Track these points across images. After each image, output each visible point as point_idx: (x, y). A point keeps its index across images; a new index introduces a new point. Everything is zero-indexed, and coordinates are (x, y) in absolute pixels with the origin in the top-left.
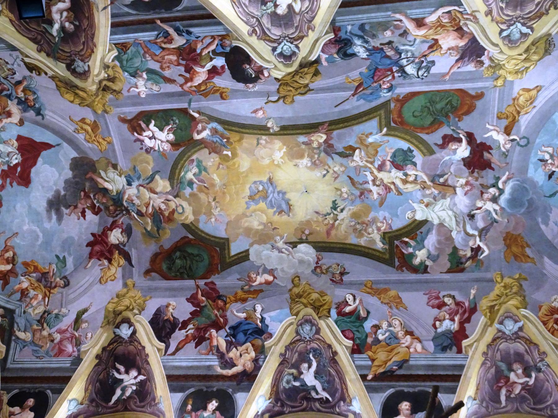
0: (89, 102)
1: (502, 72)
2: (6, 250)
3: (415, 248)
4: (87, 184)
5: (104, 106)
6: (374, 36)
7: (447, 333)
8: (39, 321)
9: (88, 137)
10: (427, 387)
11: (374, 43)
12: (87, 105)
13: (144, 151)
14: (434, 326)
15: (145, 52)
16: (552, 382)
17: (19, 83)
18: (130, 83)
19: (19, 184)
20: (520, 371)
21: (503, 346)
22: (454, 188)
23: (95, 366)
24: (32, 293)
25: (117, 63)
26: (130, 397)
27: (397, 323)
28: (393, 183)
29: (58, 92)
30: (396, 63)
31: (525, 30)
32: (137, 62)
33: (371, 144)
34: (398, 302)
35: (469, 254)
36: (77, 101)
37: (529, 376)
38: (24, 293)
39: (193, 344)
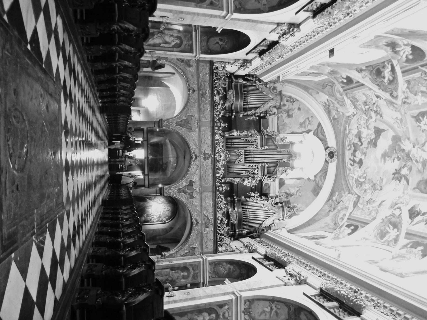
0: (398, 110)
2: (364, 173)
4: (397, 147)
5: (405, 110)
8: (367, 202)
9: (399, 125)
12: (398, 111)
13: (421, 131)
15: (418, 83)
17: (374, 104)
18: (414, 99)
19: (373, 147)
23: (382, 223)
24: (368, 191)
25: (408, 90)
26: (391, 241)
29: (387, 106)
32: (416, 88)
36: (394, 109)
38: (366, 190)
39: (424, 223)
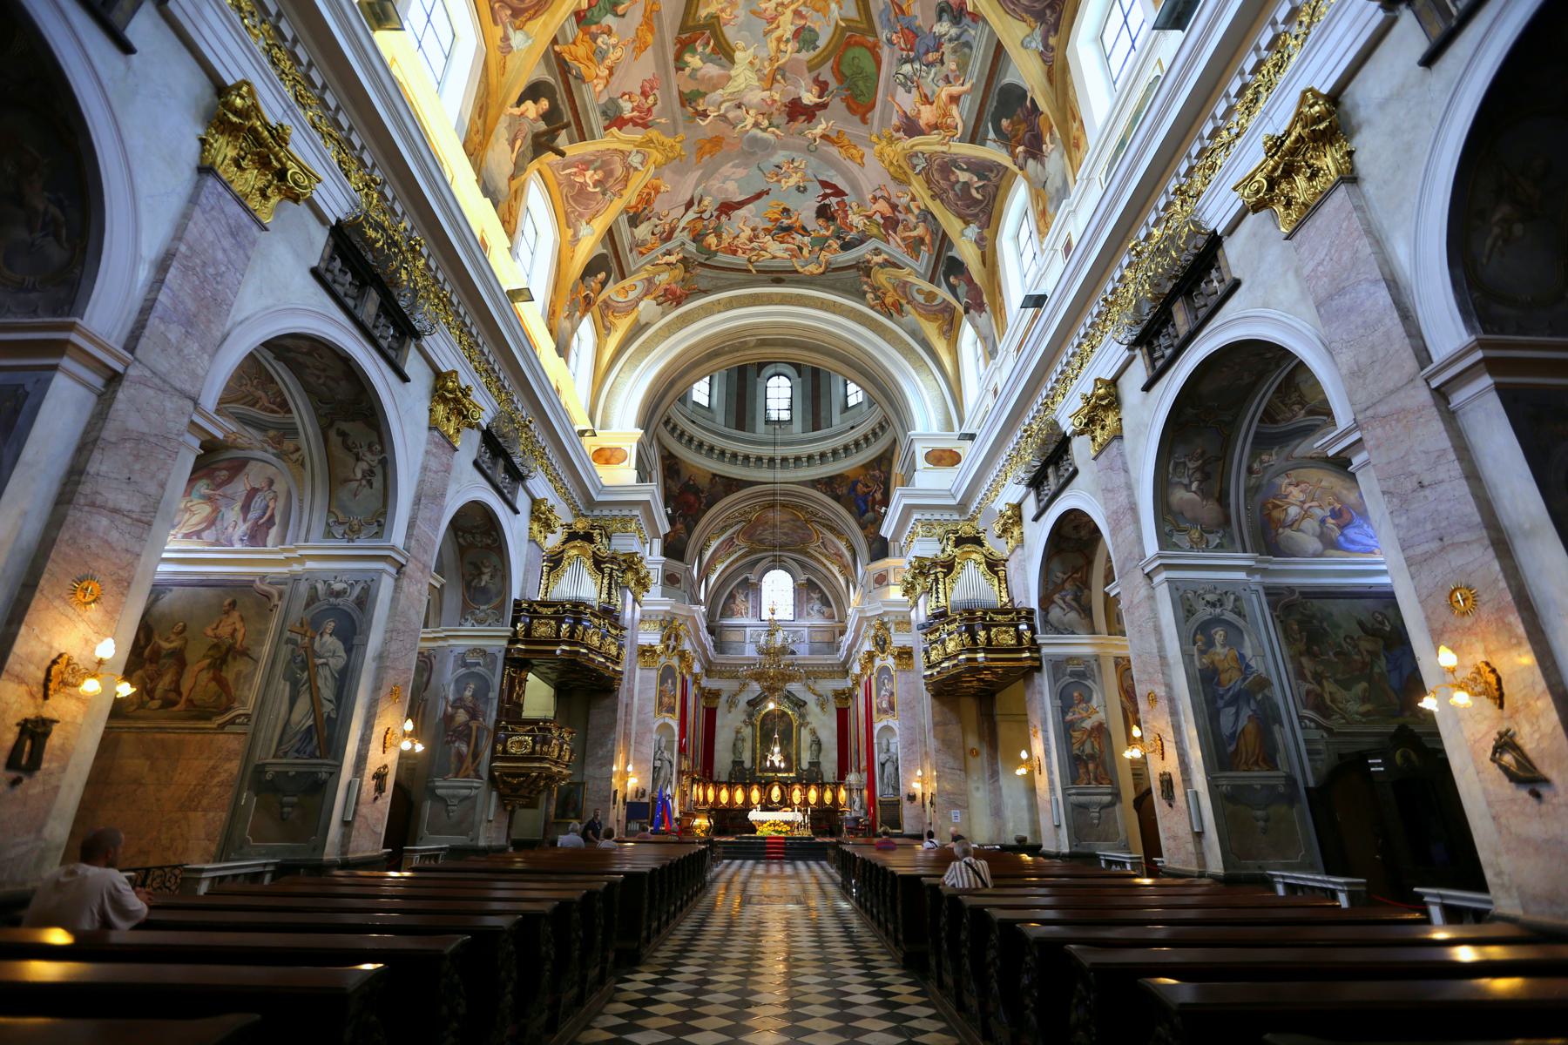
1: (884, 143)
3: (702, 54)
6: (955, 51)
7: (619, 108)
10: (568, 116)
11: (947, 48)
14: (624, 94)
16: (598, 207)
20: (596, 177)
21: (617, 159)
22: (770, 89)
27: (619, 54)
28: (778, 27)
30: (917, 58)
31: (918, 169)
33: (828, 5)
34: (640, 47)
35: (700, 108)
37: (595, 186)
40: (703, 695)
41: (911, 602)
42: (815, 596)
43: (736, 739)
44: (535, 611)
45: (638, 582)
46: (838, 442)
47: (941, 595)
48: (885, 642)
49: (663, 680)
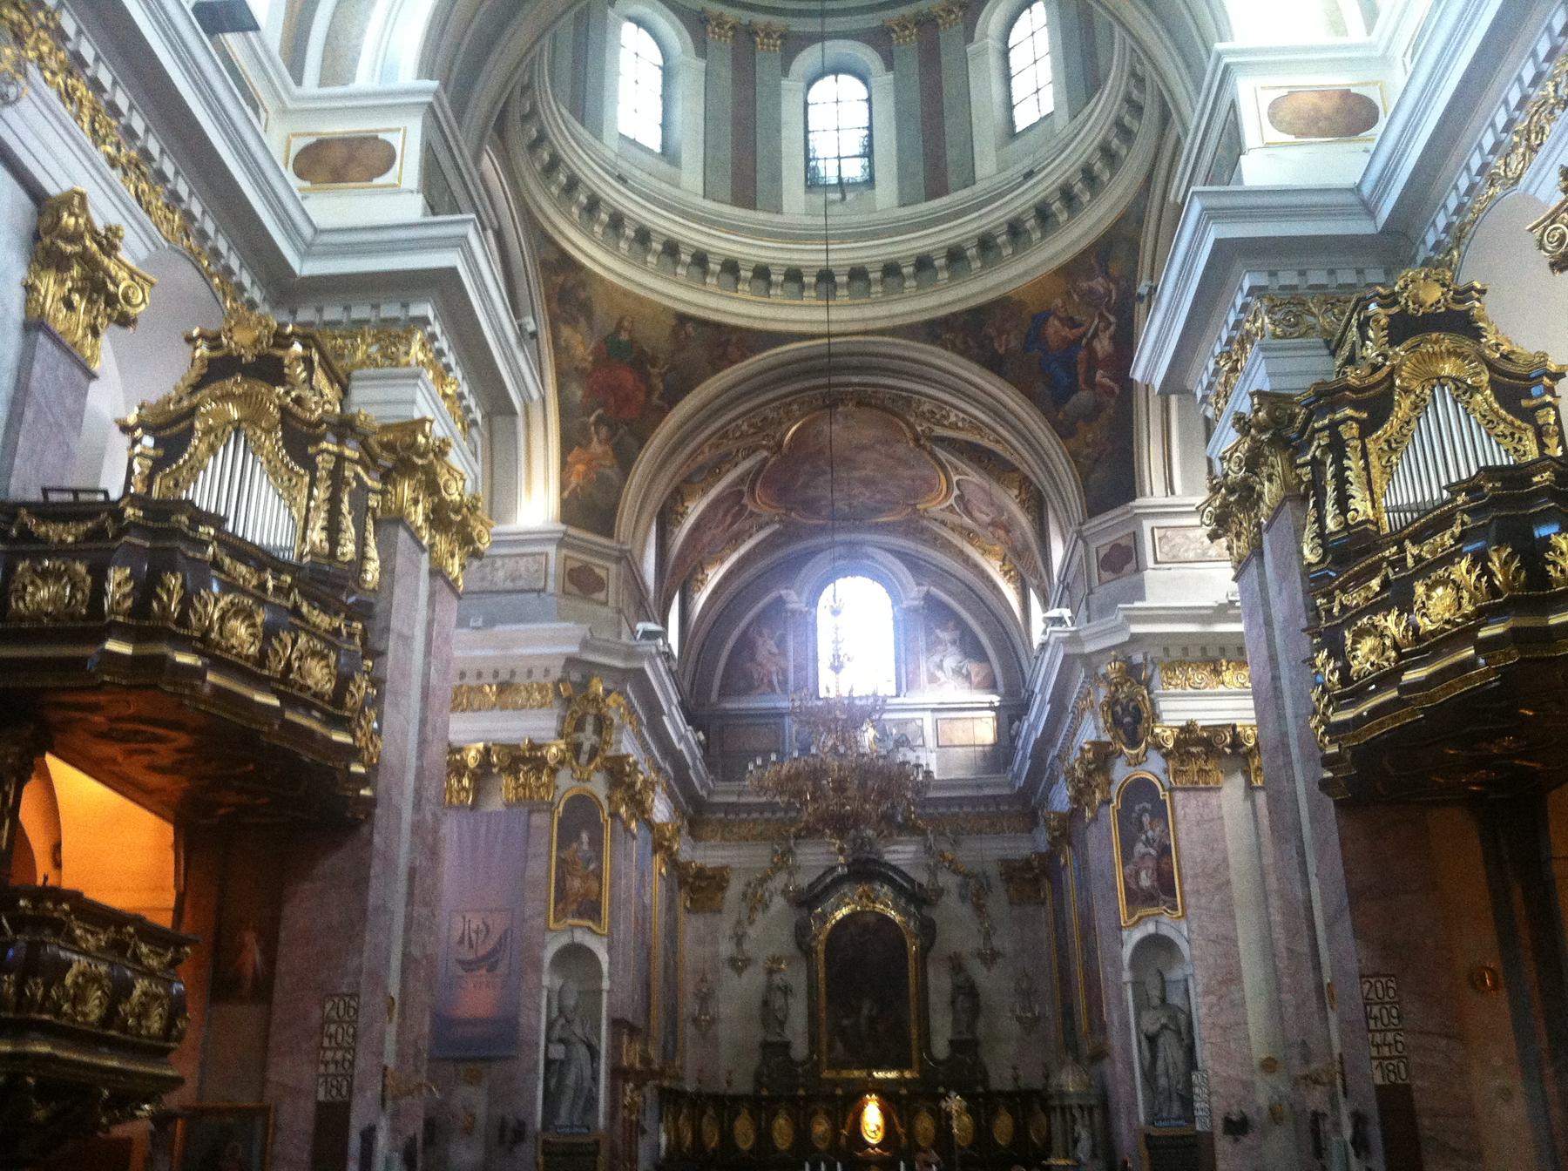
40: (682, 883)
41: (1242, 546)
42: (946, 636)
43: (770, 988)
44: (26, 535)
45: (440, 518)
46: (994, 217)
47: (1354, 490)
48: (1137, 715)
49: (567, 834)
